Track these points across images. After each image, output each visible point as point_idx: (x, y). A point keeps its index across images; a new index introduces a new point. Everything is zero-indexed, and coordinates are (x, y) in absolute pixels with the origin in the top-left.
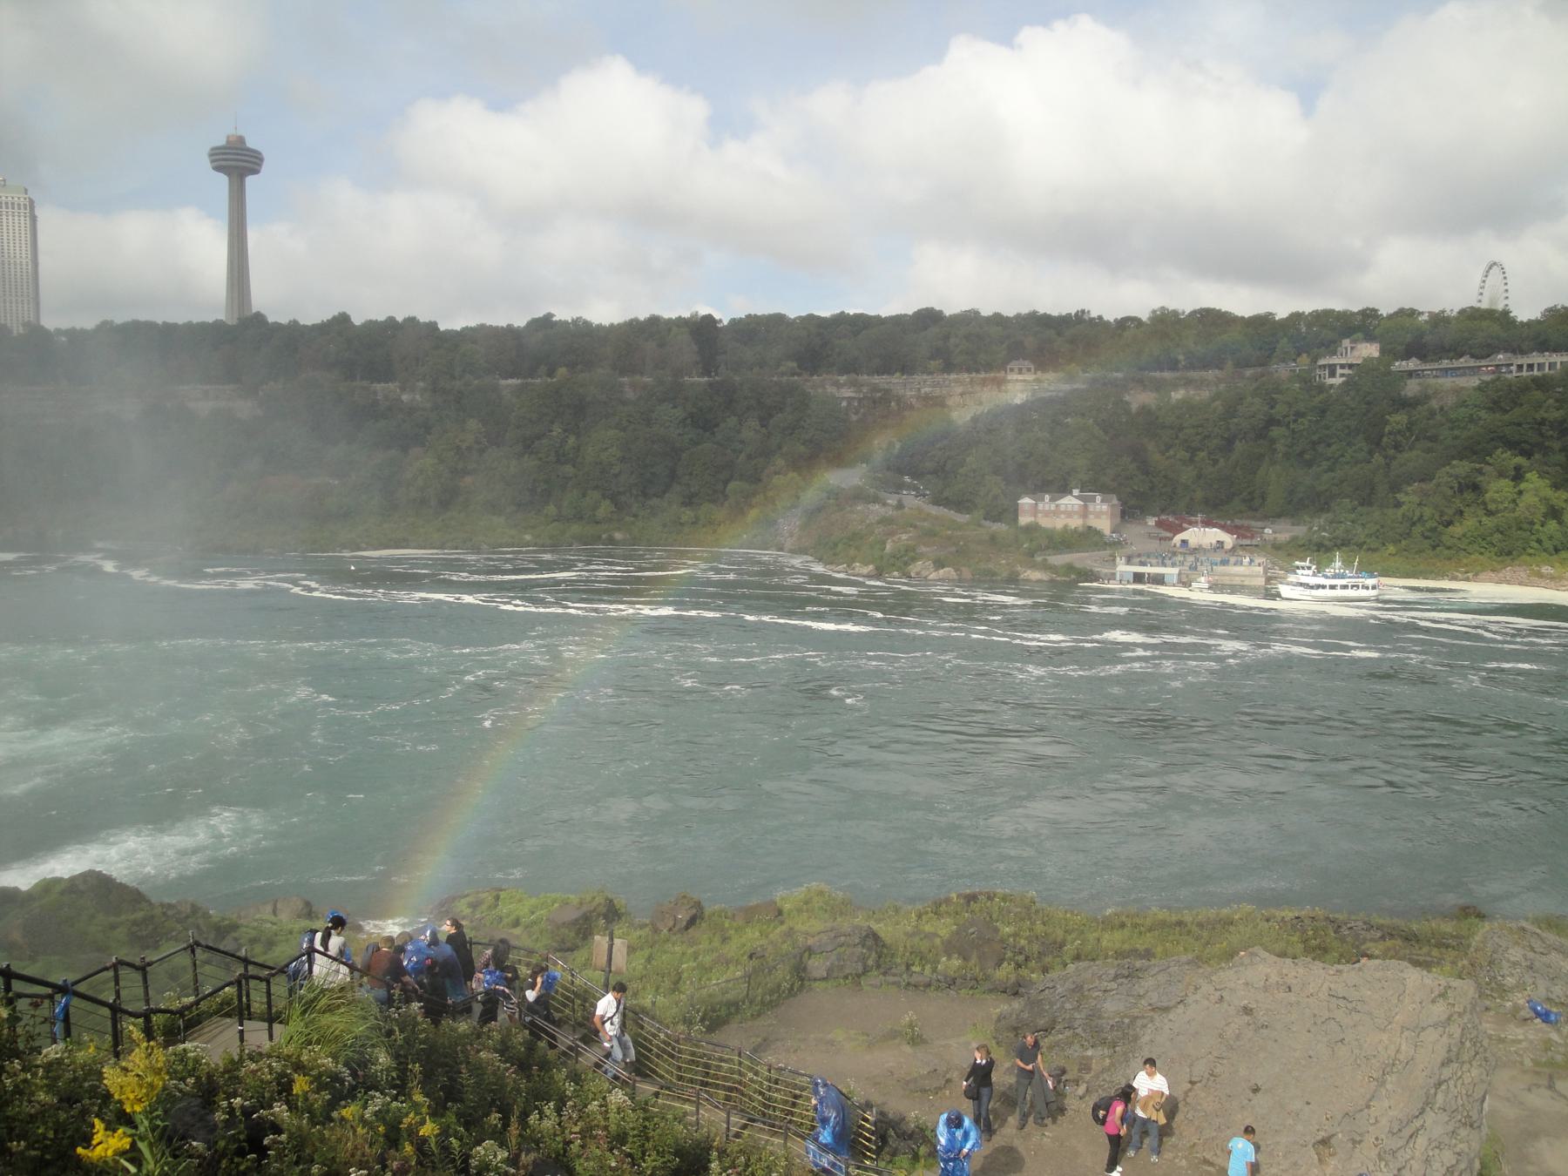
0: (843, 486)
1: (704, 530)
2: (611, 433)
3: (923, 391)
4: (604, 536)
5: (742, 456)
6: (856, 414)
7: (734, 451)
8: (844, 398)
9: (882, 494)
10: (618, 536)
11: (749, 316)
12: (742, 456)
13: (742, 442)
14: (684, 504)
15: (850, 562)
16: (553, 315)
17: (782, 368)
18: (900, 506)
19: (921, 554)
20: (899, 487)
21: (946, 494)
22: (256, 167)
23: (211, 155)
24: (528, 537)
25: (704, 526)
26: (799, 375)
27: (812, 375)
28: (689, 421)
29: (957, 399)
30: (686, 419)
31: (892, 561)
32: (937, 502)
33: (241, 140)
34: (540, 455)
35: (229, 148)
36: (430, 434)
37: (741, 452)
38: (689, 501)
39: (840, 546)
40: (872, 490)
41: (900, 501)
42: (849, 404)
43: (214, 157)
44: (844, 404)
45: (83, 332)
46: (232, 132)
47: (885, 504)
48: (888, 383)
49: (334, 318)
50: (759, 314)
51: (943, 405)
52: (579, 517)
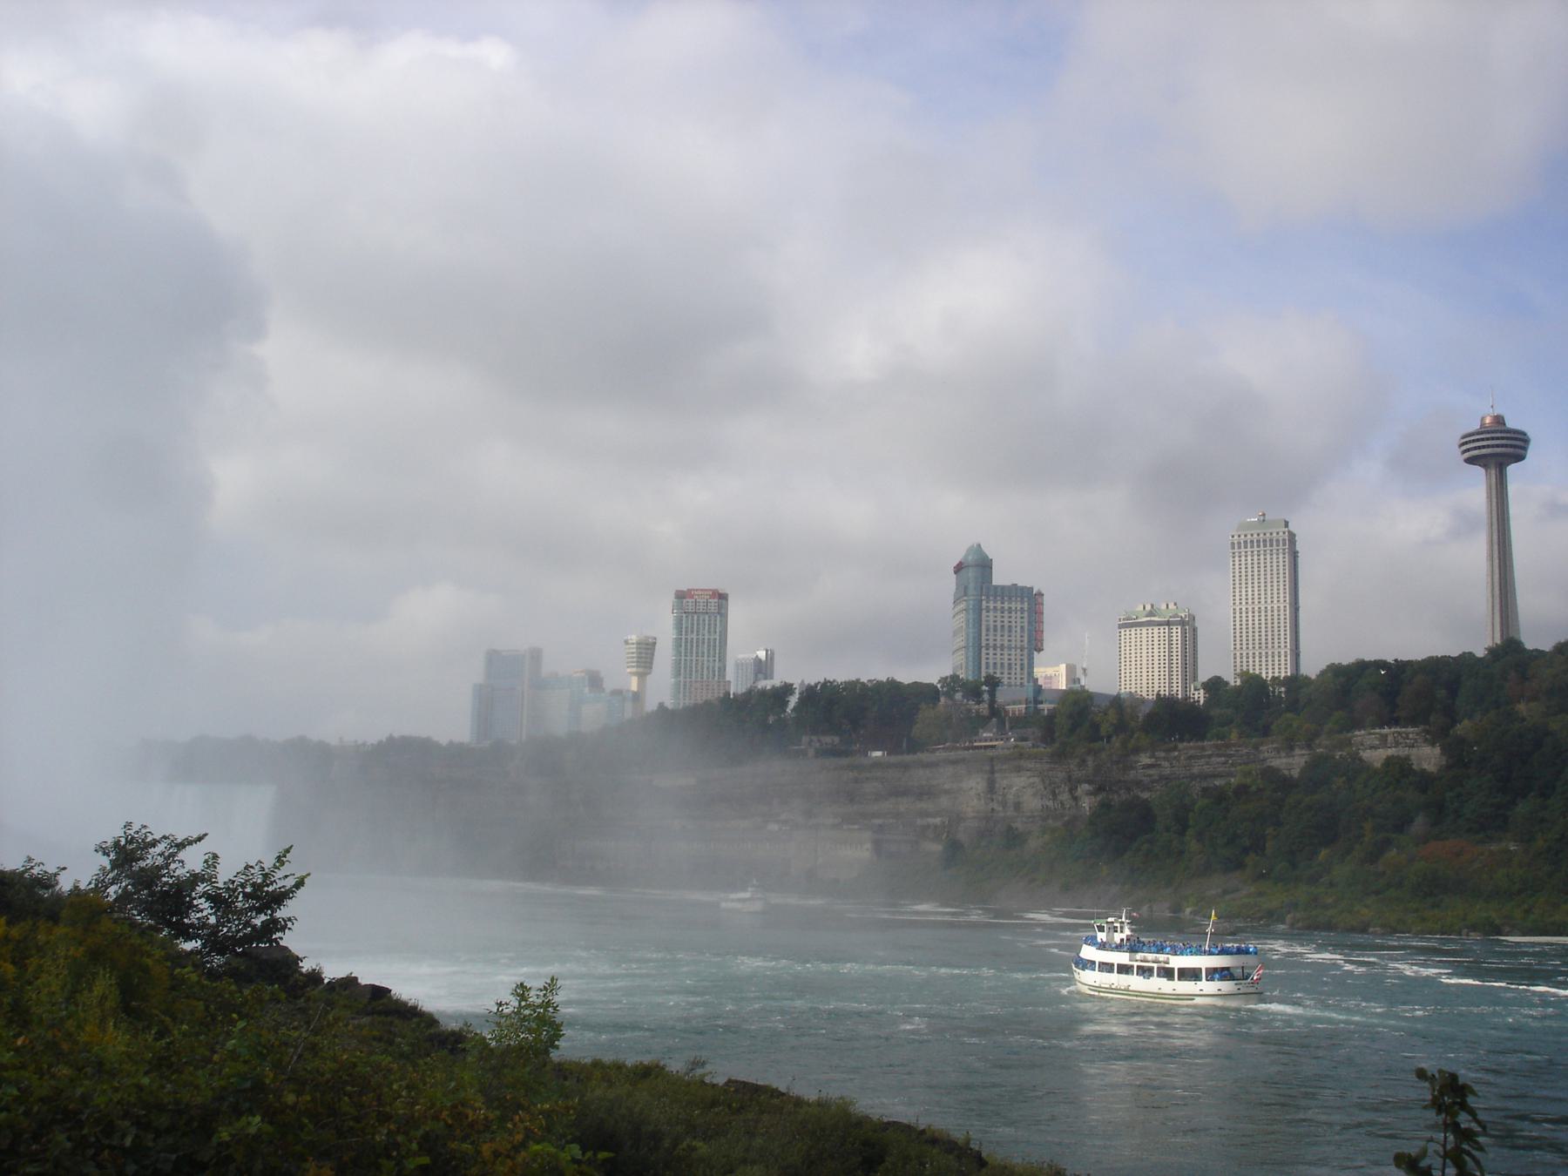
22: (1522, 452)
33: (1499, 420)
43: (1464, 447)
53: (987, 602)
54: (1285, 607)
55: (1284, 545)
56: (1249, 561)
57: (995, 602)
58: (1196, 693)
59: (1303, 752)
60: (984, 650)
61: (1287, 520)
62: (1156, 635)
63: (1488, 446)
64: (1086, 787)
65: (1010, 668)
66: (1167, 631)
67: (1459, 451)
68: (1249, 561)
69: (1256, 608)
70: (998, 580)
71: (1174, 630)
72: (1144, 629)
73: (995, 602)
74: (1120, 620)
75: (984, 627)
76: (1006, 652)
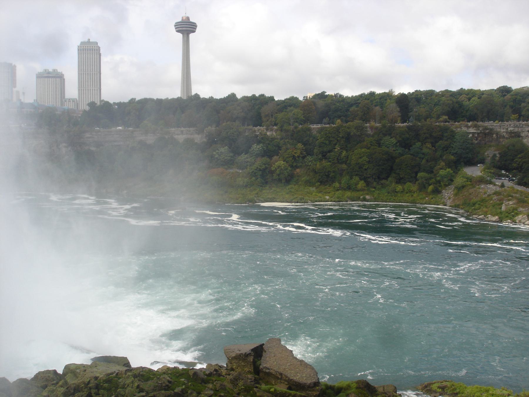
0: (473, 175)
1: (407, 195)
2: (363, 150)
3: (509, 129)
4: (361, 197)
5: (424, 161)
6: (476, 140)
7: (420, 158)
8: (471, 133)
9: (494, 180)
10: (368, 197)
11: (416, 91)
12: (424, 161)
13: (423, 154)
14: (397, 183)
15: (486, 214)
16: (326, 92)
17: (441, 119)
18: (503, 186)
19: (520, 211)
20: (500, 176)
21: (525, 180)
22: (194, 30)
23: (175, 26)
24: (327, 197)
25: (407, 193)
26: (449, 122)
27: (455, 122)
28: (398, 144)
29: (526, 133)
30: (397, 143)
31: (507, 214)
32: (519, 184)
33: (188, 18)
34: (330, 160)
35: (182, 22)
36: (280, 150)
37: (423, 159)
38: (400, 181)
39: (477, 206)
40: (488, 178)
41: (503, 183)
42: (473, 135)
44: (471, 135)
45: (124, 103)
46: (184, 15)
47: (495, 185)
48: (492, 126)
49: (229, 95)
50: (422, 90)
51: (519, 136)
52: (349, 188)
54: (97, 73)
55: (97, 51)
56: (84, 56)
58: (65, 102)
59: (152, 135)
61: (97, 42)
62: (50, 81)
63: (185, 27)
64: (64, 144)
66: (54, 80)
67: (174, 28)
68: (84, 56)
69: (87, 73)
71: (57, 79)
72: (46, 79)
74: (37, 75)
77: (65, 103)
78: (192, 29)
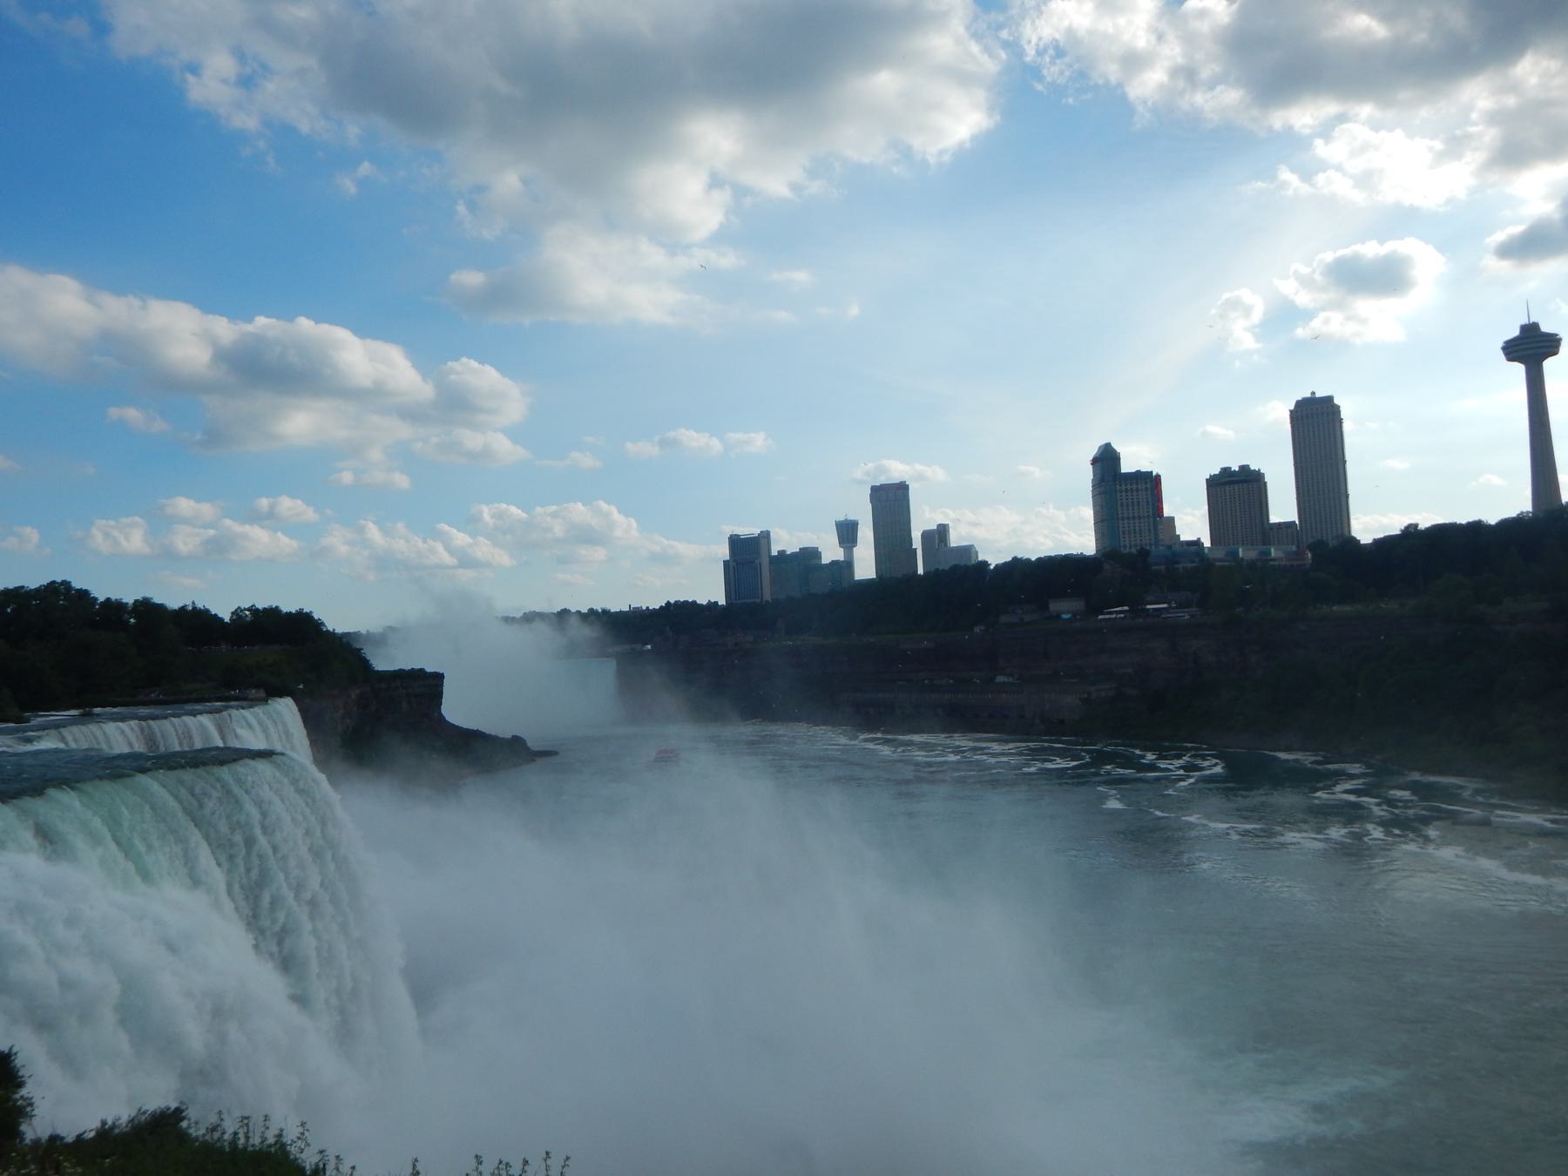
23: (1504, 349)
35: (1526, 338)
46: (1525, 321)
53: (1121, 486)
57: (1126, 485)
60: (1121, 522)
65: (1140, 533)
70: (1127, 467)
72: (1227, 488)
73: (1126, 485)
74: (1207, 480)
75: (1119, 504)
76: (1137, 521)
77: (1271, 534)
78: (1544, 350)
